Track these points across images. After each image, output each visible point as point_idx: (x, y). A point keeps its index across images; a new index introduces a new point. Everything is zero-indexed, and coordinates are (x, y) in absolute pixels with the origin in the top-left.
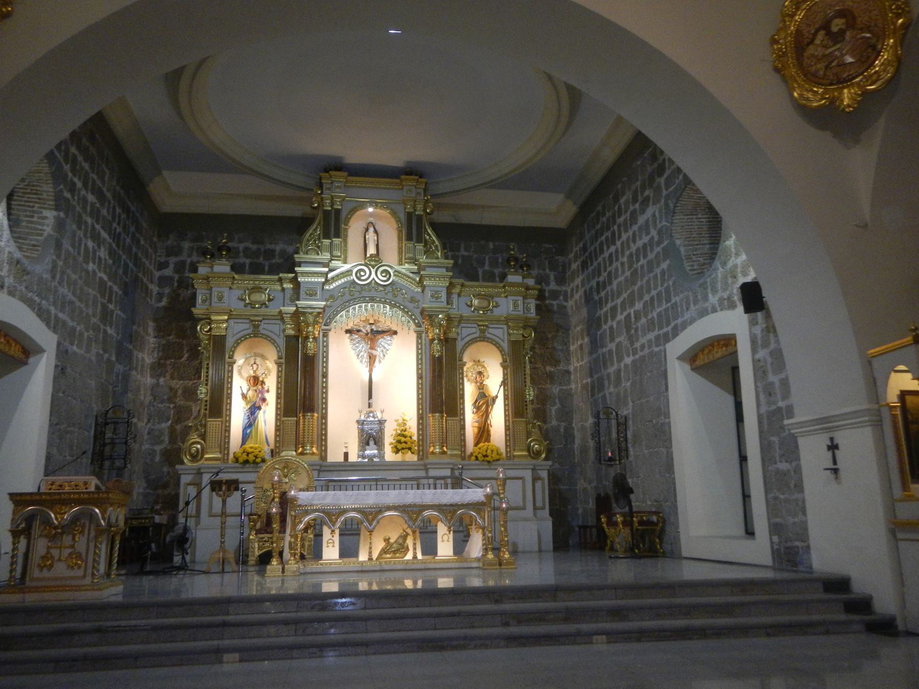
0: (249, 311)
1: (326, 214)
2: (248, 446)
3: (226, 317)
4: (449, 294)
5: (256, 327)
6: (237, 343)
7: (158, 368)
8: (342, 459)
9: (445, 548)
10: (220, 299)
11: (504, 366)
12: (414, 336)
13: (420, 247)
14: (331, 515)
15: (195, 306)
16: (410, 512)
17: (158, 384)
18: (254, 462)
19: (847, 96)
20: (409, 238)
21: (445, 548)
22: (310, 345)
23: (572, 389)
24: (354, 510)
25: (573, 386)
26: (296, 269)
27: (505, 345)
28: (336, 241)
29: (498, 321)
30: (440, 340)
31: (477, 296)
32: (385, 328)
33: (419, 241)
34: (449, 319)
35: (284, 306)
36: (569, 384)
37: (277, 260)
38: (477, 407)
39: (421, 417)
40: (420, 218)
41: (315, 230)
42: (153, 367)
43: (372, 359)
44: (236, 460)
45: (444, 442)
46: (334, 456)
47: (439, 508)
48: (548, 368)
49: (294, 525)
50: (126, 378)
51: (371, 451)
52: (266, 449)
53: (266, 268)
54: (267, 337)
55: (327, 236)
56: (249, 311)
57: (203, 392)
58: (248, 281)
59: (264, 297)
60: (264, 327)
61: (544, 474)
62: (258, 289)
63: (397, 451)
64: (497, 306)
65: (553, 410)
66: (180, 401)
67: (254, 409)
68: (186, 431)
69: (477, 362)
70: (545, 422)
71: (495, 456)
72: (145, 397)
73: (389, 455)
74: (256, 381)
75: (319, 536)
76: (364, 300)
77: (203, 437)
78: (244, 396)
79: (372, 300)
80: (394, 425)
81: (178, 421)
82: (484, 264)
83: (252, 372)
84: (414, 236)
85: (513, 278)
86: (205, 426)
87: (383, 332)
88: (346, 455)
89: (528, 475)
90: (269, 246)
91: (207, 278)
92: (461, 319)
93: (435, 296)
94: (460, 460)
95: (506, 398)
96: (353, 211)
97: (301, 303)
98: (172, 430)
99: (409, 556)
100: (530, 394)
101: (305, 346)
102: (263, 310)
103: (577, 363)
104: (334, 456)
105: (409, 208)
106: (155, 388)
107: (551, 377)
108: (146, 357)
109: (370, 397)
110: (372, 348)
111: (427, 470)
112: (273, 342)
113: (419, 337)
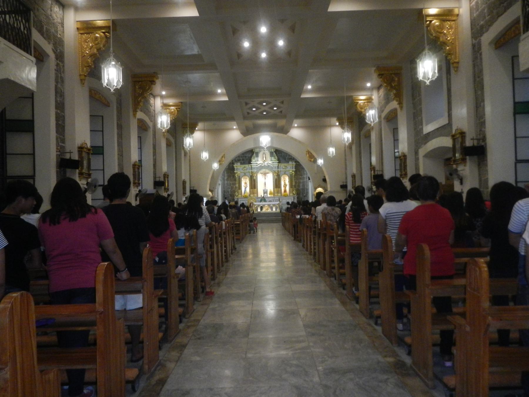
0: (243, 171)
1: (256, 153)
2: (245, 194)
3: (240, 173)
4: (278, 167)
5: (245, 174)
6: (242, 177)
7: (227, 180)
8: (260, 196)
9: (274, 210)
10: (239, 169)
11: (289, 179)
12: (272, 175)
13: (273, 158)
14: (259, 205)
15: (235, 170)
16: (269, 205)
17: (228, 183)
18: (247, 197)
19: (312, 160)
20: (271, 156)
21: (274, 210)
22: (254, 178)
23: (304, 181)
24: (262, 205)
25: (305, 180)
26: (252, 164)
27: (289, 175)
28: (258, 158)
29: (287, 171)
30: (277, 176)
31: (285, 166)
32: (267, 172)
33: (273, 157)
34: (278, 171)
35: (249, 170)
36: (304, 179)
37: (247, 158)
38: (284, 186)
39: (274, 189)
40: (273, 152)
41: (255, 154)
42: (226, 179)
43: (265, 178)
44: (244, 197)
45: (278, 193)
46: (259, 196)
47: (273, 204)
48: (300, 177)
49: (254, 207)
50: (225, 183)
51: (266, 195)
52: (248, 195)
53: (245, 160)
54: (247, 176)
55: (256, 157)
56: (243, 171)
57: (237, 185)
58: (243, 166)
59: (245, 169)
60: (246, 174)
61: (296, 198)
62: (245, 167)
63: (270, 194)
64: (287, 168)
65: (301, 185)
66: (232, 185)
67: (246, 188)
68: (235, 192)
69: (284, 178)
70: (299, 187)
71: (287, 195)
72: (226, 185)
73: (269, 196)
74: (246, 183)
75: (257, 208)
76: (263, 168)
77: (238, 193)
78: (244, 186)
79: (265, 168)
80: (269, 190)
81: (232, 189)
82: (287, 156)
83: (245, 182)
84: (272, 155)
85: (290, 163)
86: (238, 191)
87: (267, 173)
88: (261, 196)
89: (293, 198)
90: (245, 155)
91: (237, 166)
92: (281, 171)
93: (275, 168)
94: (280, 196)
95: (289, 185)
96: (261, 151)
97: (253, 170)
98: (231, 191)
99: (269, 211)
100: (294, 184)
101: (253, 178)
102: (246, 171)
103: (305, 176)
104: (259, 196)
105: (271, 151)
106: (227, 184)
107: (301, 178)
108: (226, 178)
109: (265, 185)
110: (265, 176)
111: (274, 198)
112: (248, 177)
113: (273, 175)
